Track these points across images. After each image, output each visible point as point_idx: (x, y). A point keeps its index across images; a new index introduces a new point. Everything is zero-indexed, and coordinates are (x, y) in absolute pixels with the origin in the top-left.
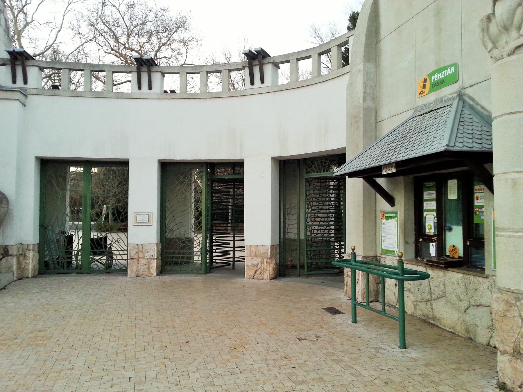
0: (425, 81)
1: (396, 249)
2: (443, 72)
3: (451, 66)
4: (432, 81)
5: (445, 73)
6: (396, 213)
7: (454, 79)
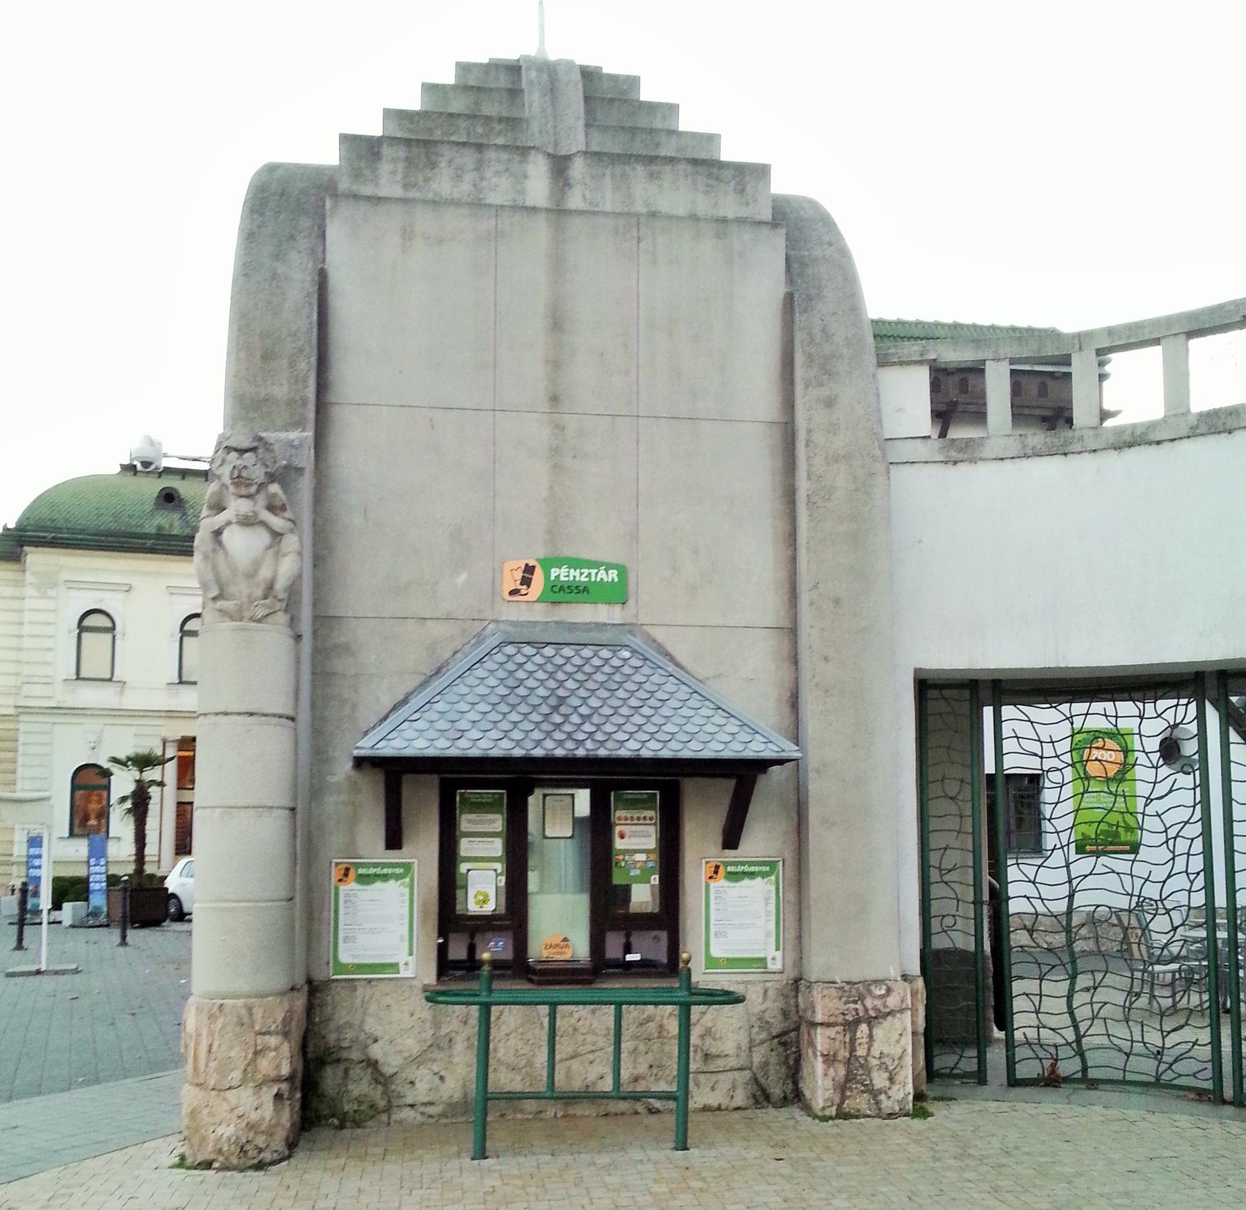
0: (529, 570)
1: (401, 955)
2: (586, 571)
3: (609, 567)
4: (553, 578)
5: (590, 574)
6: (407, 867)
7: (618, 594)
